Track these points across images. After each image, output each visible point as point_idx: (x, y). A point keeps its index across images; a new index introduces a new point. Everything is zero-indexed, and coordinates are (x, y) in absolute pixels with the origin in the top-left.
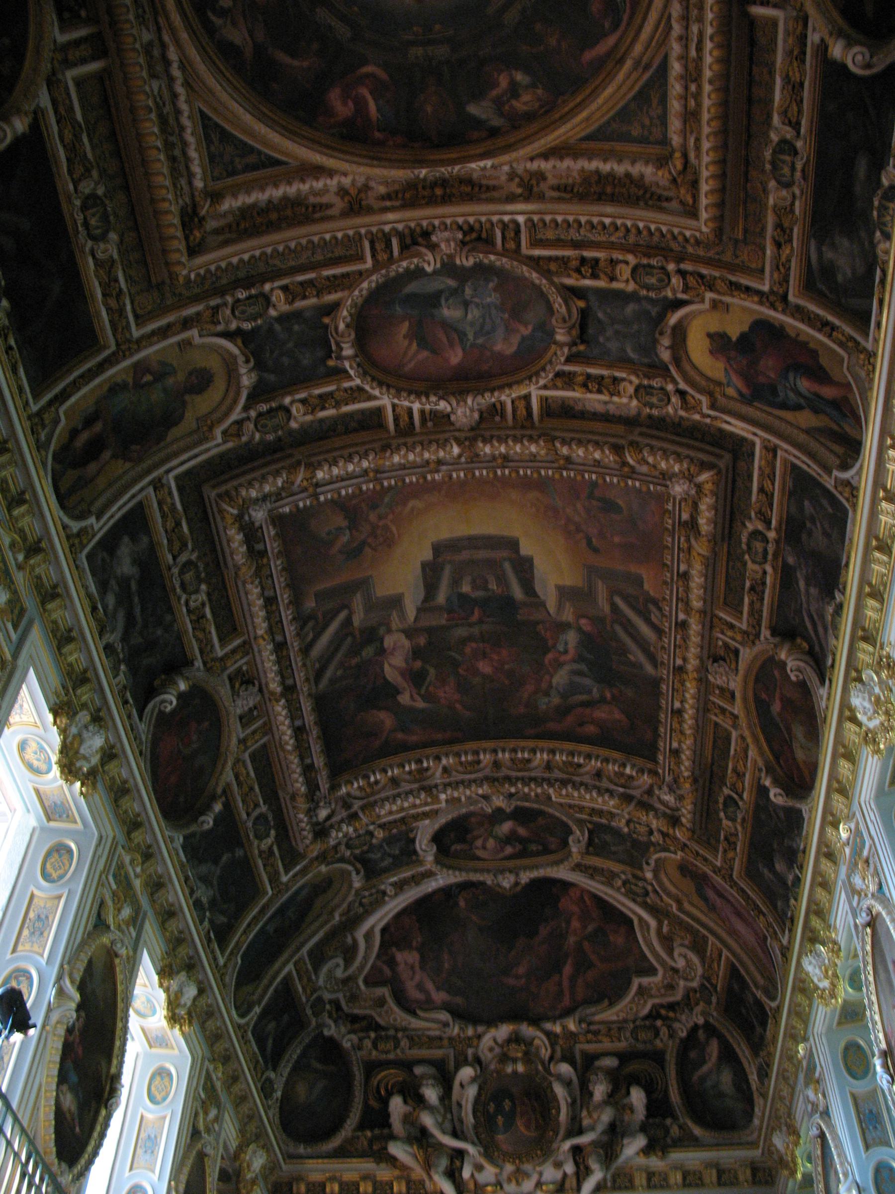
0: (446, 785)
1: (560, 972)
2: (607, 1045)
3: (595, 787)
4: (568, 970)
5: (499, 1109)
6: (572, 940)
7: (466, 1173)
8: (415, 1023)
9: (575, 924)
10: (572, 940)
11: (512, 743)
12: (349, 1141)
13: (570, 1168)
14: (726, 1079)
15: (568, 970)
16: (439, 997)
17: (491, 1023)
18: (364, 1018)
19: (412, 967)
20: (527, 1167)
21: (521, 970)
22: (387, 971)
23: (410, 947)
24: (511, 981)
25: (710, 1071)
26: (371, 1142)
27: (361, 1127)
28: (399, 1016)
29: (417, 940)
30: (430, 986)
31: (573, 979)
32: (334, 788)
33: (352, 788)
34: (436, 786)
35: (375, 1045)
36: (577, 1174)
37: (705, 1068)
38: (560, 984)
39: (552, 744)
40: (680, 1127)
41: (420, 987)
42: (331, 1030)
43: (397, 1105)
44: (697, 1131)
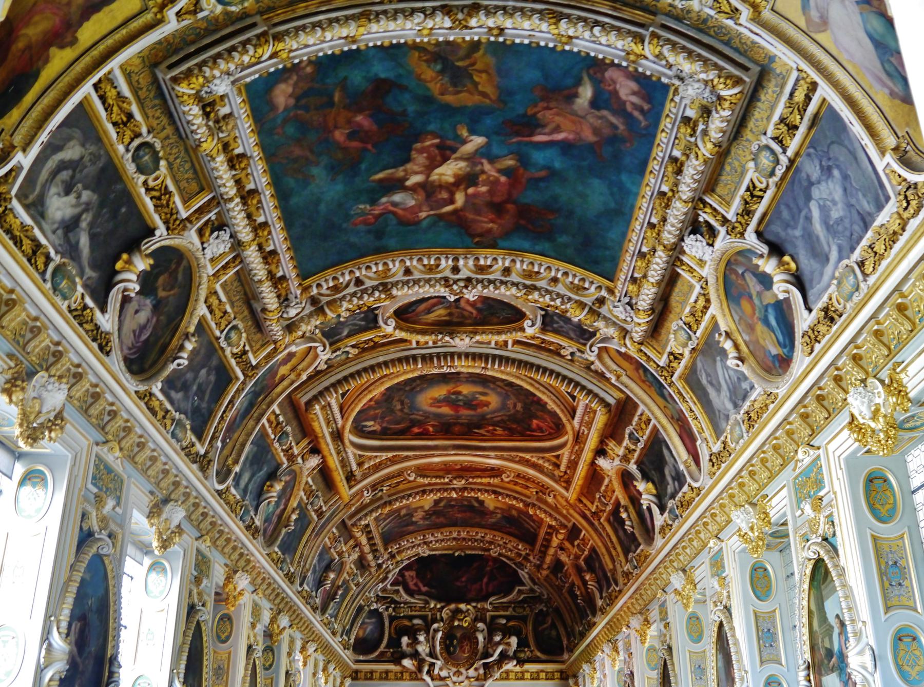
0: (437, 541)
1: (482, 581)
2: (502, 613)
3: (505, 548)
4: (485, 580)
5: (451, 644)
6: (488, 568)
7: (436, 671)
8: (413, 601)
9: (490, 563)
10: (488, 568)
11: (468, 529)
12: (382, 653)
13: (481, 671)
14: (554, 633)
15: (485, 580)
16: (424, 589)
17: (448, 603)
18: (389, 597)
19: (412, 577)
20: (463, 670)
21: (463, 579)
22: (400, 579)
23: (412, 570)
24: (458, 584)
25: (546, 628)
26: (392, 654)
27: (387, 646)
28: (406, 597)
29: (415, 567)
30: (421, 585)
31: (487, 584)
32: (386, 549)
33: (394, 548)
34: (431, 542)
35: (394, 610)
36: (485, 673)
37: (545, 626)
38: (481, 585)
39: (487, 531)
40: (531, 652)
41: (416, 585)
42: (374, 606)
43: (405, 640)
44: (539, 654)
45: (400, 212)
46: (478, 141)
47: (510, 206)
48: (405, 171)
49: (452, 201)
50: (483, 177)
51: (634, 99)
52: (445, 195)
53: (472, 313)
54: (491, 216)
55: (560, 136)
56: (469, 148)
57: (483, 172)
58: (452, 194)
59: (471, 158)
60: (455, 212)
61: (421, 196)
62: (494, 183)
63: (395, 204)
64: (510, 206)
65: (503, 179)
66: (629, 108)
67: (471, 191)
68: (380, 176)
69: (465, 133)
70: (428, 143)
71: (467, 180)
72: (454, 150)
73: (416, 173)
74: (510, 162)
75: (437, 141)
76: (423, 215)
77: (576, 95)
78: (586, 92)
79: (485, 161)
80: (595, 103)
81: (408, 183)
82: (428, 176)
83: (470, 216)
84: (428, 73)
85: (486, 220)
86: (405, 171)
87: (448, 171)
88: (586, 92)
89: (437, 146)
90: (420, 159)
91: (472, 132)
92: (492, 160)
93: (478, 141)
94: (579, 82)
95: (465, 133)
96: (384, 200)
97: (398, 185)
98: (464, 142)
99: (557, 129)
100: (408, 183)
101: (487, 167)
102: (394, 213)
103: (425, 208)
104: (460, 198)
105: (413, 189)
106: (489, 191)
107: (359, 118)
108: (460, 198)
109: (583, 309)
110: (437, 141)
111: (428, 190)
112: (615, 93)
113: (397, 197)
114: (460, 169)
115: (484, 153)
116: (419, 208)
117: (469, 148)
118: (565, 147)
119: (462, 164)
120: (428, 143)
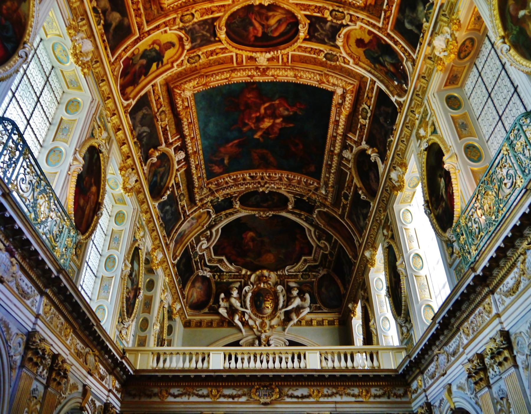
45: (286, 105)
46: (256, 136)
47: (242, 108)
48: (282, 125)
49: (266, 109)
50: (254, 121)
51: (213, 168)
53: (255, 19)
54: (249, 102)
55: (230, 144)
56: (259, 134)
57: (254, 123)
58: (265, 112)
59: (258, 129)
62: (250, 118)
63: (287, 110)
64: (242, 108)
65: (247, 121)
66: (214, 165)
67: (258, 114)
68: (291, 125)
69: (261, 139)
70: (273, 136)
71: (260, 120)
72: (264, 133)
73: (278, 124)
75: (270, 136)
76: (277, 102)
77: (229, 159)
78: (226, 162)
79: (254, 128)
80: (223, 160)
81: (281, 119)
82: (274, 122)
83: (258, 101)
84: (272, 159)
85: (252, 99)
87: (267, 124)
88: (226, 162)
89: (270, 135)
90: (276, 130)
91: (258, 139)
92: (251, 128)
93: (256, 136)
94: (229, 163)
95: (261, 139)
96: (291, 113)
97: (286, 119)
98: (261, 136)
99: (232, 146)
100: (281, 119)
101: (253, 126)
102: (289, 106)
103: (276, 105)
104: (262, 111)
105: (280, 116)
106: (251, 114)
107: (294, 149)
108: (262, 111)
110: (270, 136)
111: (274, 116)
112: (218, 166)
113: (286, 113)
114: (262, 124)
115: (255, 132)
116: (280, 105)
117: (259, 134)
118: (228, 141)
119: (262, 126)
120: (273, 136)
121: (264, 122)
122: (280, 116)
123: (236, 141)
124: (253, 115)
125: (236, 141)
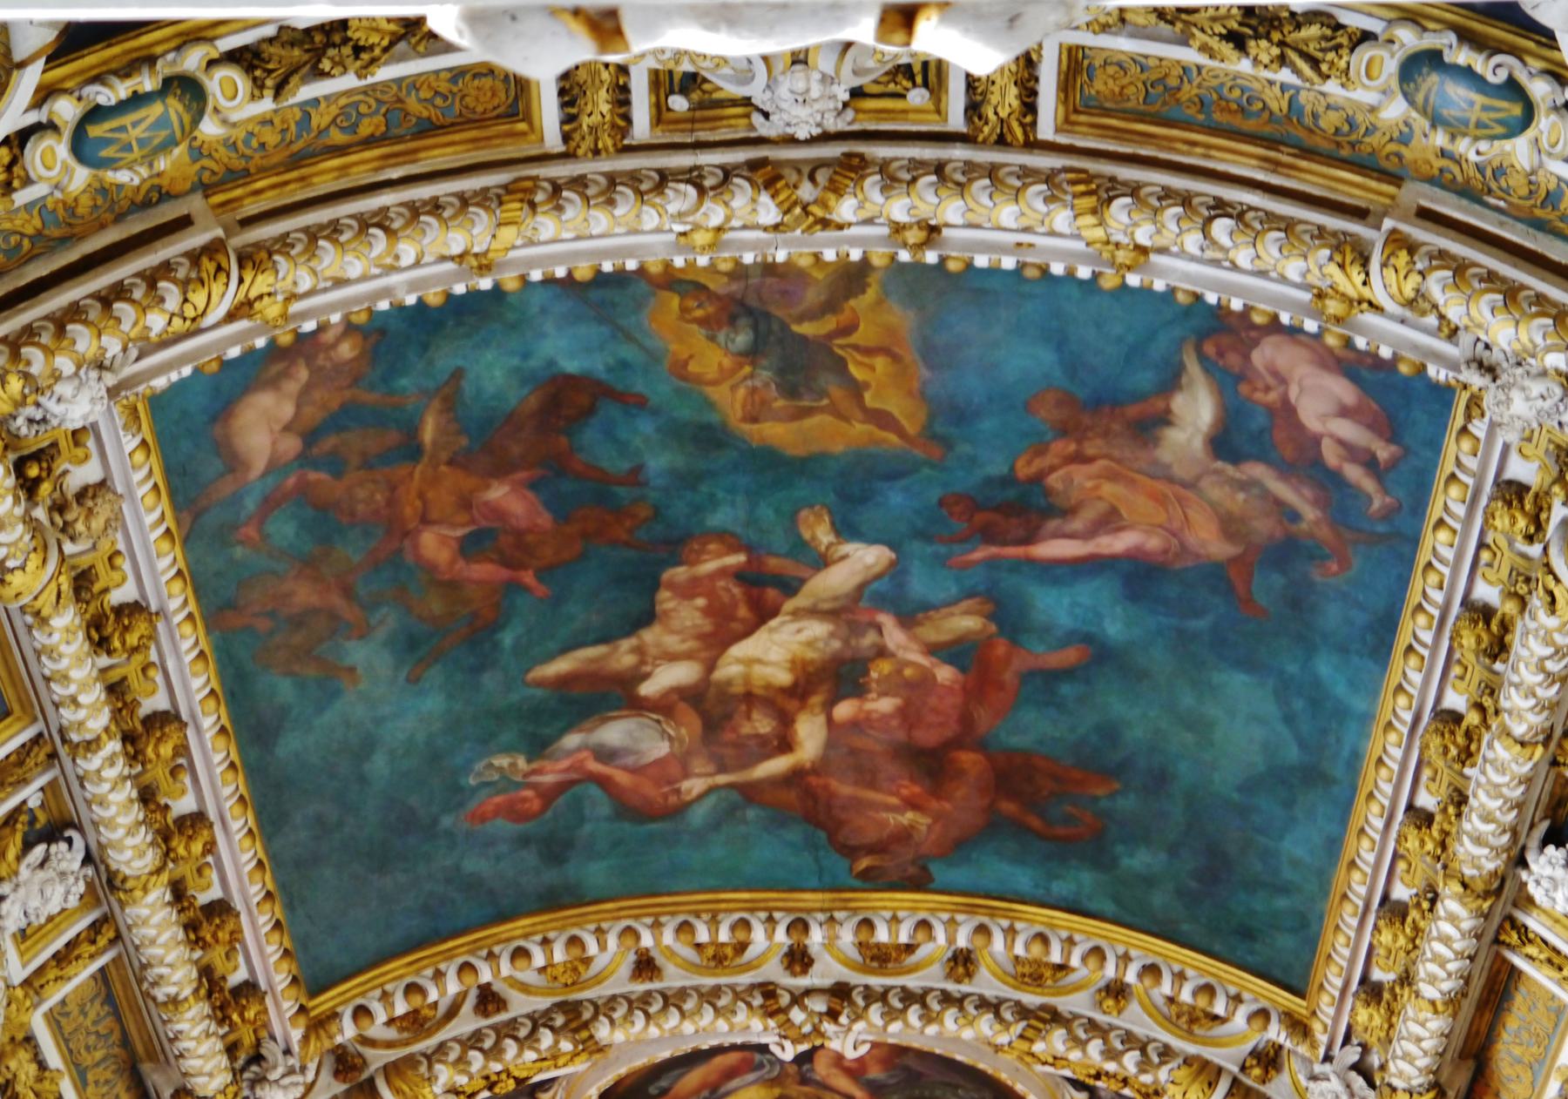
45: (622, 778)
47: (968, 759)
48: (640, 651)
49: (785, 744)
51: (1347, 430)
52: (763, 724)
55: (1118, 543)
56: (836, 580)
57: (882, 652)
58: (786, 721)
59: (843, 612)
60: (796, 777)
61: (689, 728)
62: (917, 688)
63: (606, 754)
64: (968, 759)
65: (945, 674)
67: (844, 710)
69: (823, 535)
70: (709, 566)
72: (790, 587)
73: (672, 657)
74: (965, 622)
75: (737, 559)
76: (694, 786)
77: (1165, 419)
79: (887, 620)
81: (647, 689)
82: (711, 666)
83: (844, 789)
85: (894, 800)
86: (640, 651)
89: (739, 575)
91: (847, 530)
92: (907, 620)
94: (1172, 381)
95: (823, 535)
96: (572, 740)
98: (823, 562)
99: (1110, 521)
100: (647, 689)
101: (894, 637)
102: (603, 782)
103: (699, 765)
105: (663, 707)
106: (902, 712)
107: (498, 493)
108: (810, 735)
109: (1212, 1085)
110: (737, 559)
112: (1287, 410)
113: (614, 733)
114: (810, 644)
116: (680, 764)
117: (836, 580)
119: (817, 629)
120: (709, 566)
121: (798, 665)
122: (663, 707)
123: (1053, 549)
124: (885, 705)
125: (1053, 549)
